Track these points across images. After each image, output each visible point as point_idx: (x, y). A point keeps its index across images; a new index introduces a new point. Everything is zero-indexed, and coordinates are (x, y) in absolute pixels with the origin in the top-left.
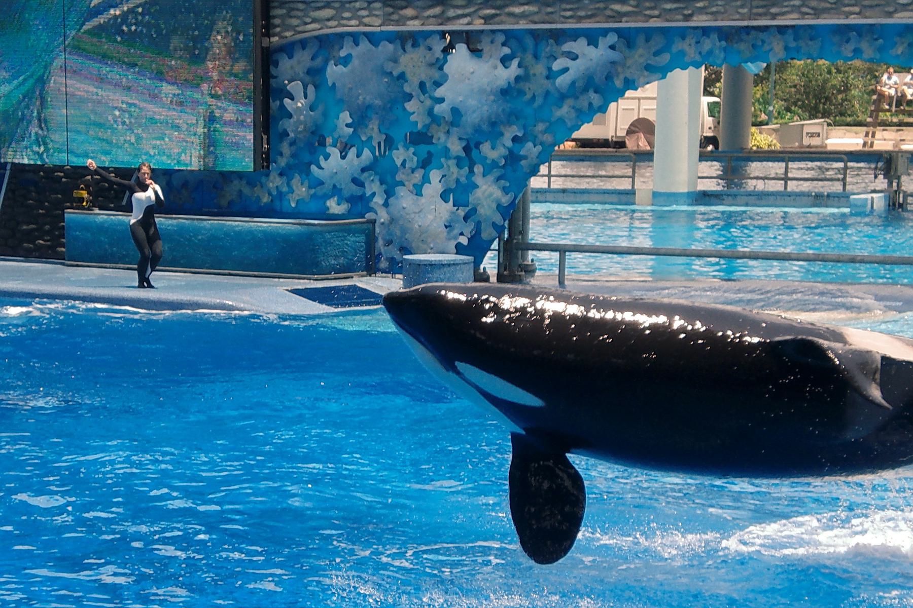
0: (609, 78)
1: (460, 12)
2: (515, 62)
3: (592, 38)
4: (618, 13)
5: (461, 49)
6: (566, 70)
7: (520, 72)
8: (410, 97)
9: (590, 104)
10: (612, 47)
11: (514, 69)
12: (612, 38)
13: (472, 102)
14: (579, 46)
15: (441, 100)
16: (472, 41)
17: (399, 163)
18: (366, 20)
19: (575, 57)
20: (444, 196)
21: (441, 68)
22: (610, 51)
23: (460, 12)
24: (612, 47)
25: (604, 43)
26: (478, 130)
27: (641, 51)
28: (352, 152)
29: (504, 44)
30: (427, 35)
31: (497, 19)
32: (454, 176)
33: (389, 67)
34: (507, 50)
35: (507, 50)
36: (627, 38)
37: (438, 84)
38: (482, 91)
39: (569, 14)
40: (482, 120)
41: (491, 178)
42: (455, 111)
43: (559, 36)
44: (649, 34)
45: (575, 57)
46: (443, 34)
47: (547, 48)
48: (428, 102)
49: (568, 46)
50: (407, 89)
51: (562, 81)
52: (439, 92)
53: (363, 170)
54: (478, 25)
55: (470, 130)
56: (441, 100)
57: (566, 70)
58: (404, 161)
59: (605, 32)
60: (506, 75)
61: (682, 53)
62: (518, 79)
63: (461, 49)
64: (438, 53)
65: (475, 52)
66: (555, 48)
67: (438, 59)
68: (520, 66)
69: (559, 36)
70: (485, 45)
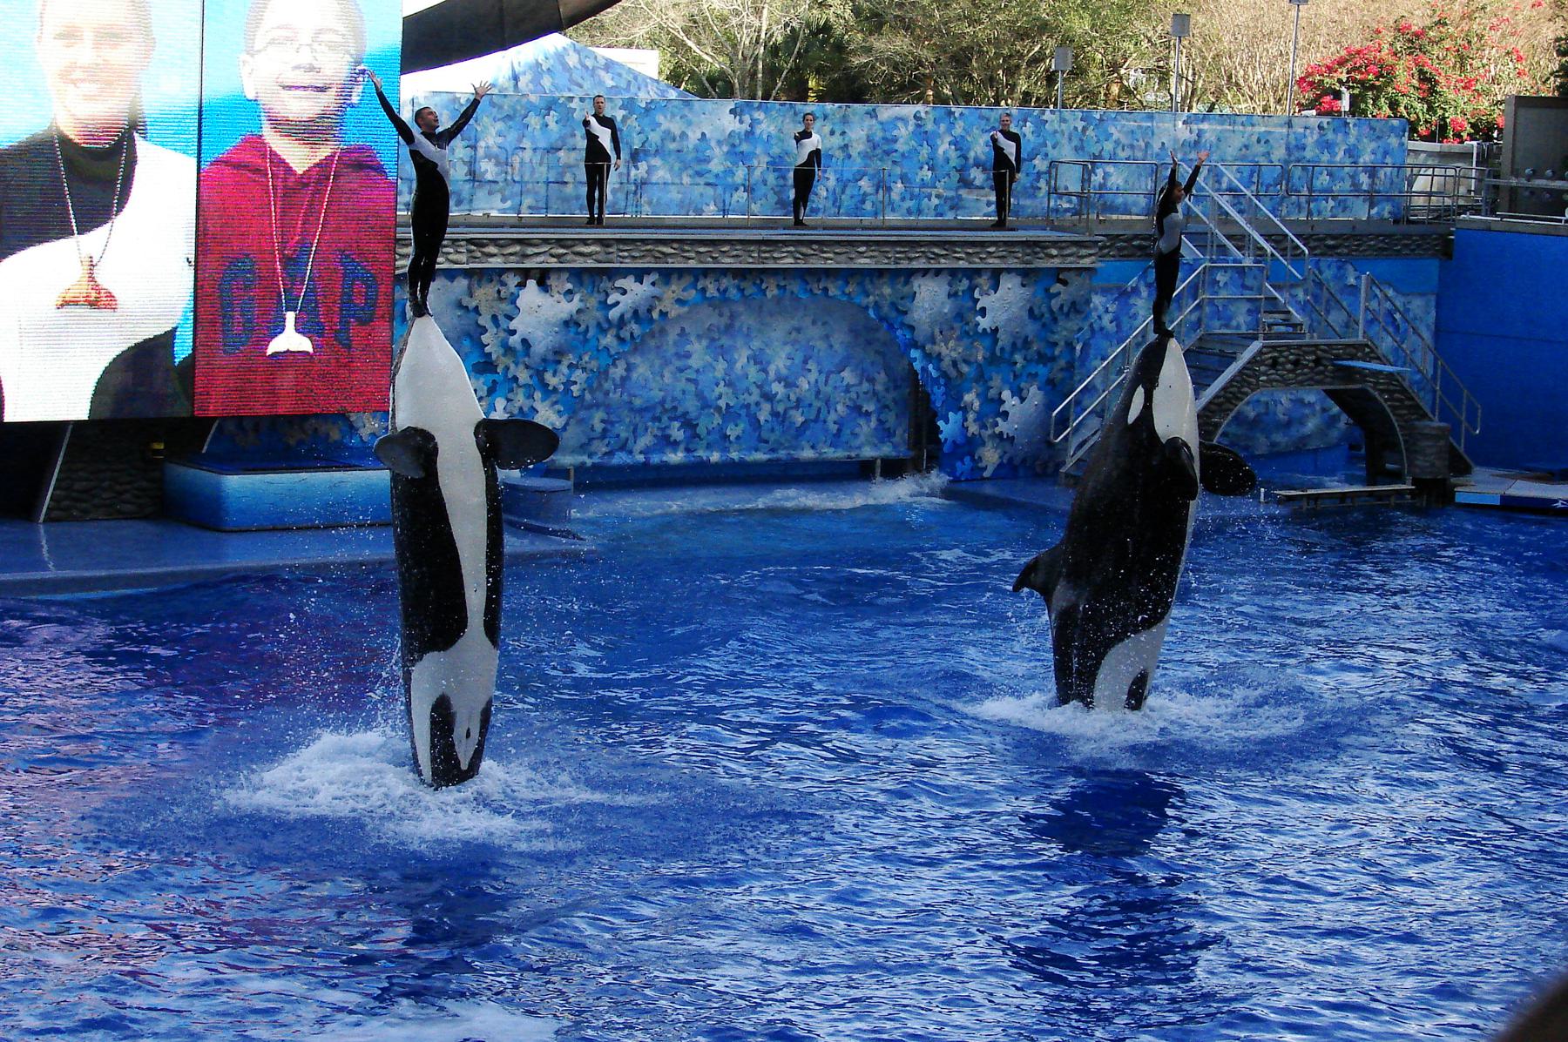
0: (649, 311)
1: (536, 250)
2: (577, 297)
3: (640, 274)
4: (663, 253)
5: (532, 284)
6: (617, 303)
7: (581, 305)
8: (484, 330)
9: (632, 334)
10: (653, 284)
12: (654, 277)
13: (540, 333)
14: (628, 283)
15: (513, 332)
16: (543, 278)
18: (450, 257)
19: (624, 292)
21: (513, 302)
22: (652, 288)
23: (536, 251)
24: (653, 284)
25: (648, 280)
26: (544, 360)
27: (674, 287)
29: (568, 280)
30: (501, 272)
31: (568, 258)
32: (518, 405)
33: (466, 301)
34: (569, 286)
35: (569, 286)
36: (667, 275)
37: (511, 318)
38: (548, 323)
39: (626, 254)
40: (547, 350)
41: (547, 403)
42: (525, 342)
43: (613, 274)
44: (681, 272)
45: (624, 292)
46: (516, 271)
47: (605, 284)
48: (502, 334)
49: (620, 283)
50: (481, 321)
51: (614, 314)
52: (513, 325)
54: (553, 263)
55: (537, 359)
56: (513, 332)
57: (617, 303)
59: (648, 271)
60: (567, 308)
61: (704, 290)
62: (579, 311)
63: (532, 284)
64: (512, 289)
65: (543, 284)
66: (610, 285)
68: (581, 301)
69: (613, 274)
70: (552, 281)
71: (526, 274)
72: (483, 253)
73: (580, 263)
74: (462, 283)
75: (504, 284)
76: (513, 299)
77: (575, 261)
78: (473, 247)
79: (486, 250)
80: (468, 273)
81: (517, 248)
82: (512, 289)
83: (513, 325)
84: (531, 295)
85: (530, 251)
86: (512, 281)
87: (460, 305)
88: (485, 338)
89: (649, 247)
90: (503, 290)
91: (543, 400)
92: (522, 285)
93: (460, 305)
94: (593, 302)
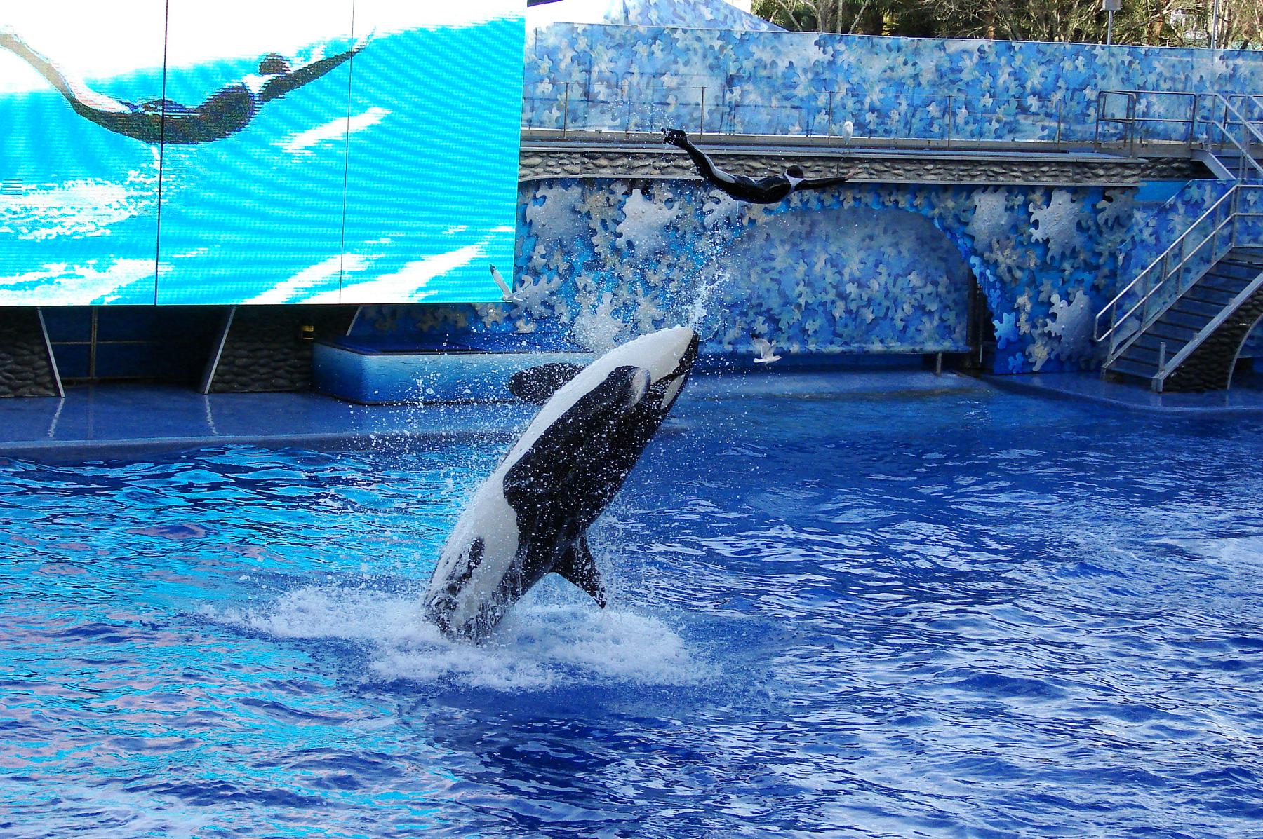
1: (641, 163)
2: (676, 205)
5: (637, 192)
6: (712, 211)
8: (595, 232)
11: (676, 210)
16: (647, 188)
17: (581, 286)
18: (565, 168)
19: (717, 201)
20: (615, 313)
21: (620, 209)
23: (641, 163)
28: (544, 279)
31: (670, 170)
33: (579, 207)
35: (670, 195)
38: (650, 227)
45: (717, 201)
46: (624, 181)
51: (708, 221)
53: (552, 293)
54: (656, 175)
56: (620, 235)
57: (712, 211)
58: (586, 285)
63: (637, 192)
64: (620, 197)
67: (620, 201)
71: (632, 183)
72: (595, 165)
73: (679, 175)
74: (576, 191)
75: (613, 192)
76: (620, 206)
77: (674, 173)
78: (586, 160)
79: (597, 162)
80: (583, 182)
81: (625, 161)
82: (620, 197)
83: (619, 229)
84: (636, 201)
85: (636, 163)
86: (620, 189)
87: (574, 210)
88: (595, 240)
89: (740, 162)
90: (612, 198)
91: (645, 296)
92: (629, 194)
93: (574, 210)
94: (690, 210)
